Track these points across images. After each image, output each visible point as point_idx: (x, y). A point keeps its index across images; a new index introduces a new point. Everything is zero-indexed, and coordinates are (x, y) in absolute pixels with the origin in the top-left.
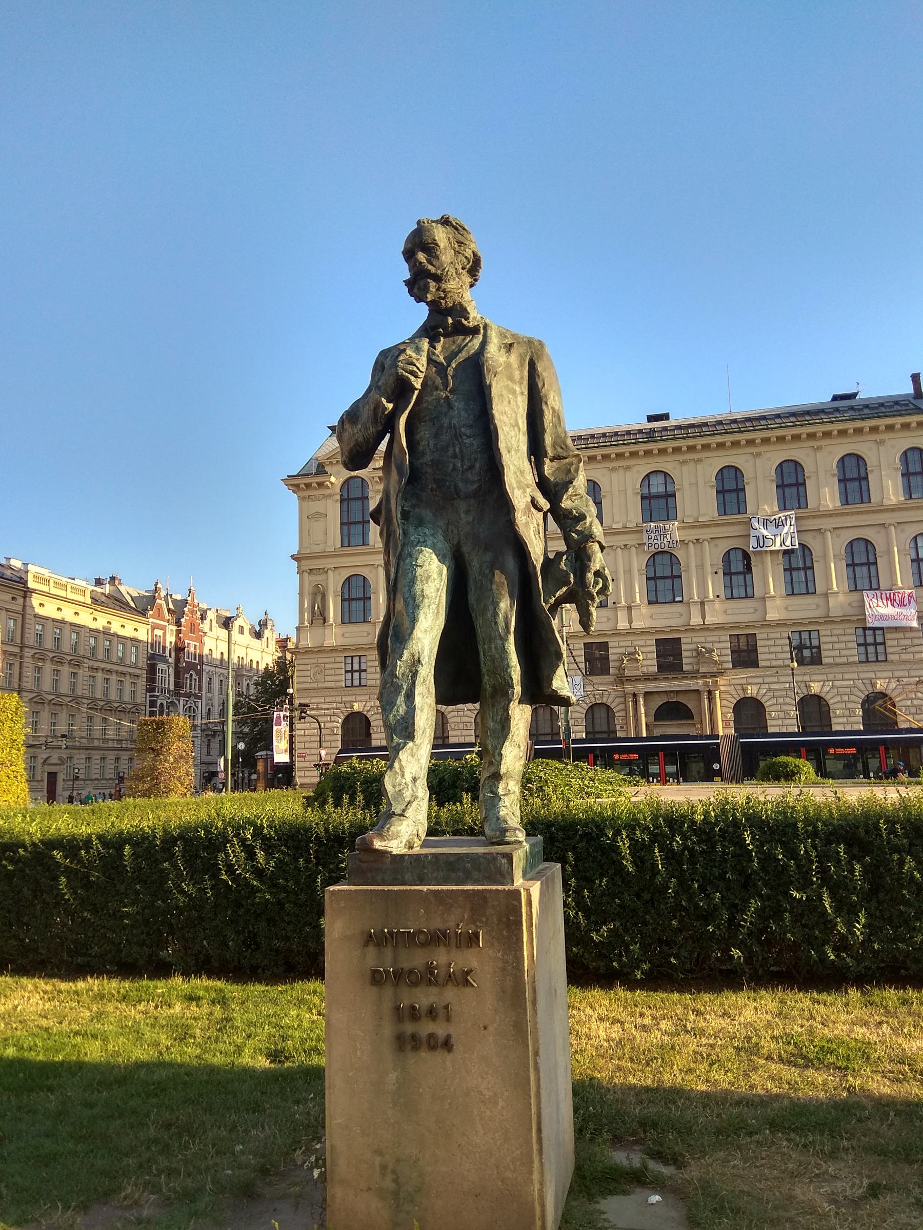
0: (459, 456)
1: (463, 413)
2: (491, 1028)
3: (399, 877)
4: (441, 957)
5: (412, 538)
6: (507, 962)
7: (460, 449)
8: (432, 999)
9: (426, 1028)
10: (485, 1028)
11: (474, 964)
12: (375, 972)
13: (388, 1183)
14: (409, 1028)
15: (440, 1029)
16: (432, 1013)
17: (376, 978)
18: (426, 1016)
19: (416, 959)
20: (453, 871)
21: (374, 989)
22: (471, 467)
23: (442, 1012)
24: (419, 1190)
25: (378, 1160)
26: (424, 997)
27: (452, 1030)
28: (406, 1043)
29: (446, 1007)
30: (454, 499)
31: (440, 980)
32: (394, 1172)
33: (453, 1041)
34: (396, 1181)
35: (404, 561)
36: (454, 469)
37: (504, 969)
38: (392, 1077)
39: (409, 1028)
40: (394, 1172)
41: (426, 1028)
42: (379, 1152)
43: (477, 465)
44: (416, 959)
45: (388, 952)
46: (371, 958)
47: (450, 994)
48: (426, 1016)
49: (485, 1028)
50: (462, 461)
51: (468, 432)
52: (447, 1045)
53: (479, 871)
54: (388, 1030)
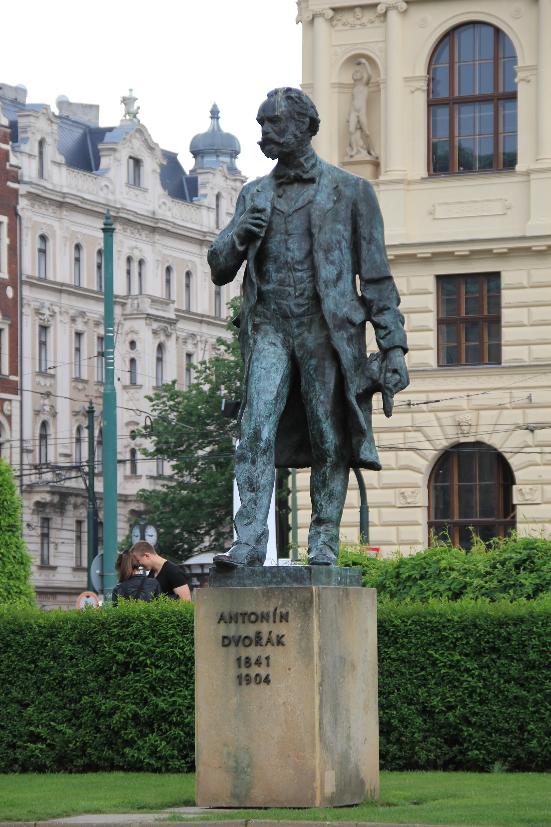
0: (293, 284)
1: (297, 253)
2: (293, 670)
3: (242, 581)
4: (264, 628)
5: (259, 346)
6: (303, 630)
7: (294, 279)
8: (258, 654)
9: (254, 671)
10: (289, 669)
11: (283, 631)
12: (224, 638)
13: (232, 764)
14: (244, 671)
15: (263, 671)
16: (258, 663)
17: (226, 642)
18: (256, 664)
19: (250, 630)
20: (275, 577)
21: (224, 649)
22: (302, 295)
23: (264, 662)
24: (249, 766)
25: (226, 750)
26: (254, 652)
27: (270, 671)
28: (243, 680)
29: (267, 658)
30: (289, 317)
31: (264, 641)
32: (235, 756)
33: (270, 678)
34: (236, 761)
35: (253, 363)
36: (290, 294)
37: (302, 634)
38: (235, 700)
39: (244, 671)
40: (235, 756)
41: (254, 671)
42: (225, 745)
43: (306, 293)
44: (250, 630)
45: (233, 625)
46: (223, 630)
47: (269, 650)
48: (256, 664)
49: (289, 669)
50: (295, 289)
51: (299, 267)
52: (267, 680)
53: (291, 577)
54: (233, 672)
